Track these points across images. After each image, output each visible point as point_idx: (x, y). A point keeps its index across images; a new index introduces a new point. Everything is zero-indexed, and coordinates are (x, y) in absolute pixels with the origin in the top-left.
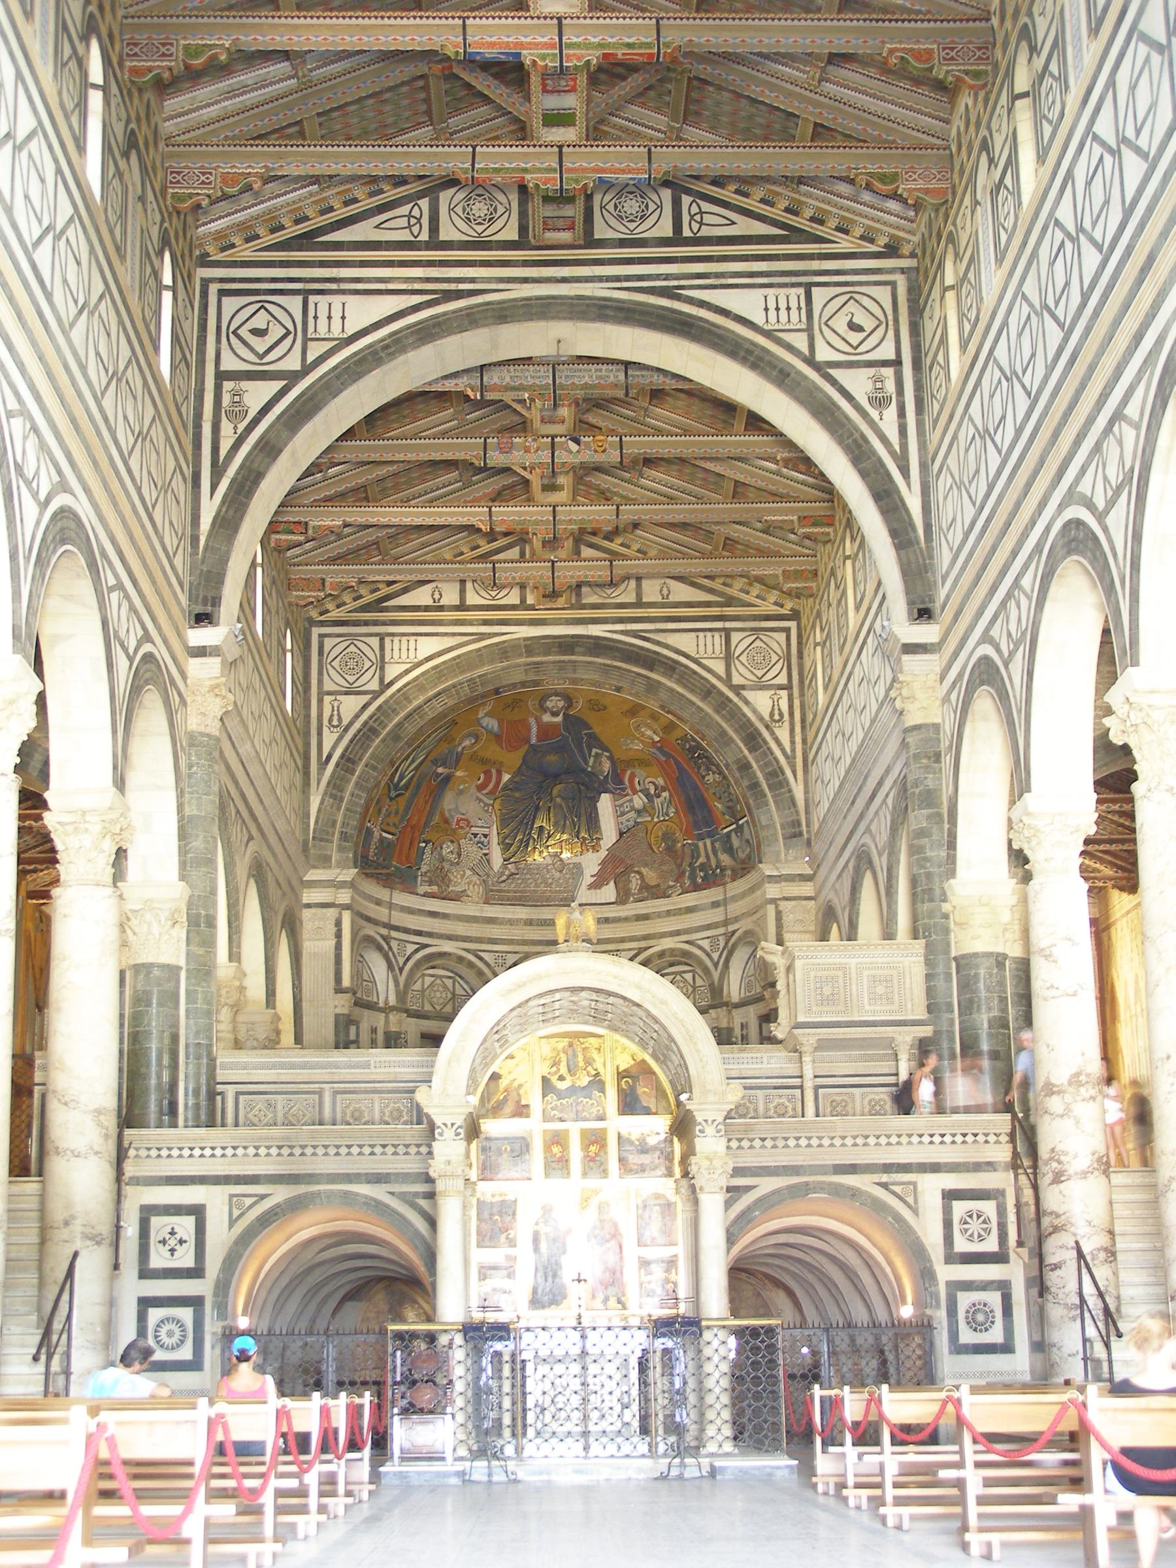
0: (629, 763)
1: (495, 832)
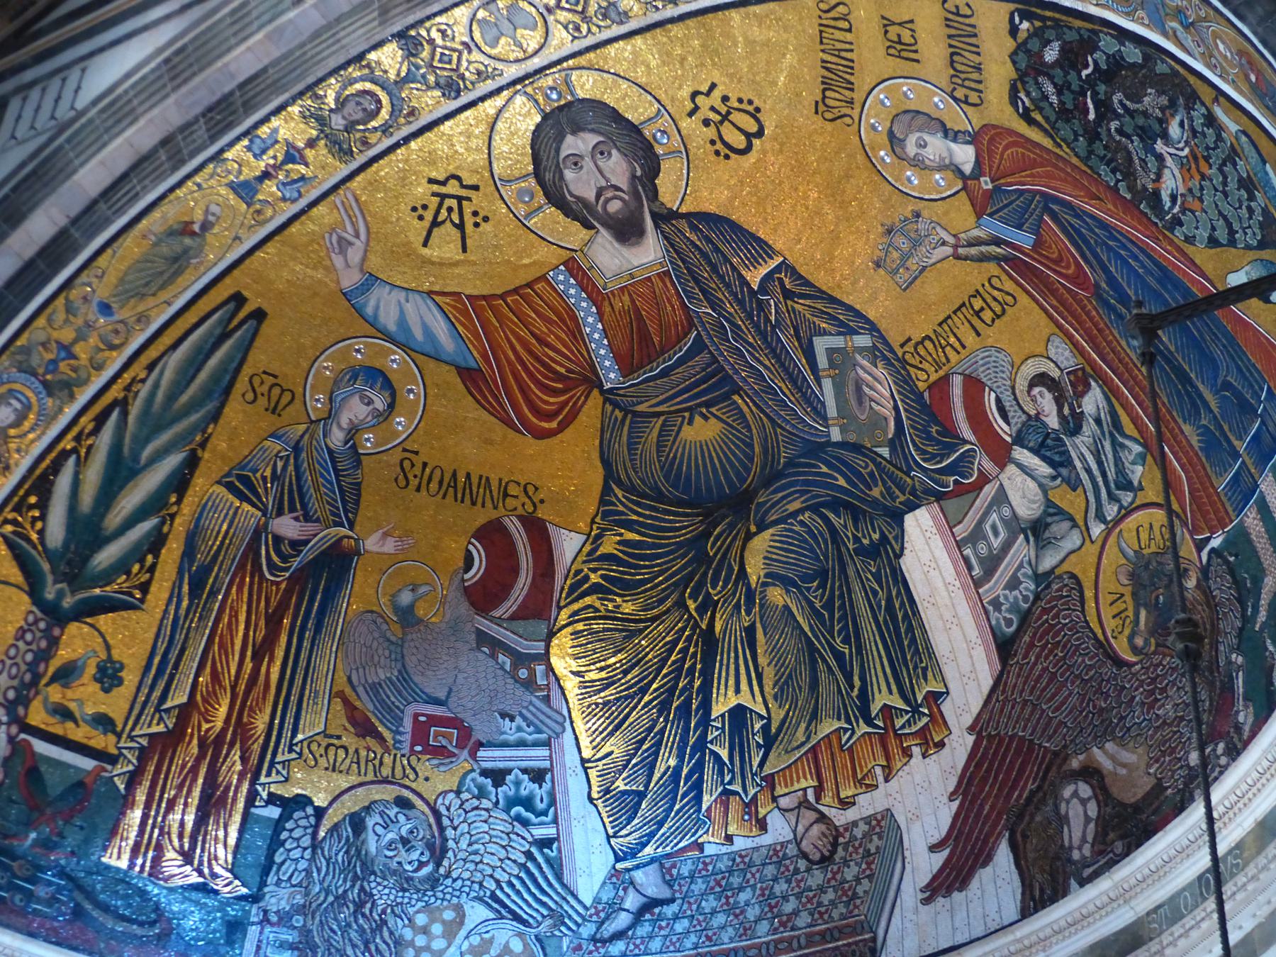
1: (572, 759)
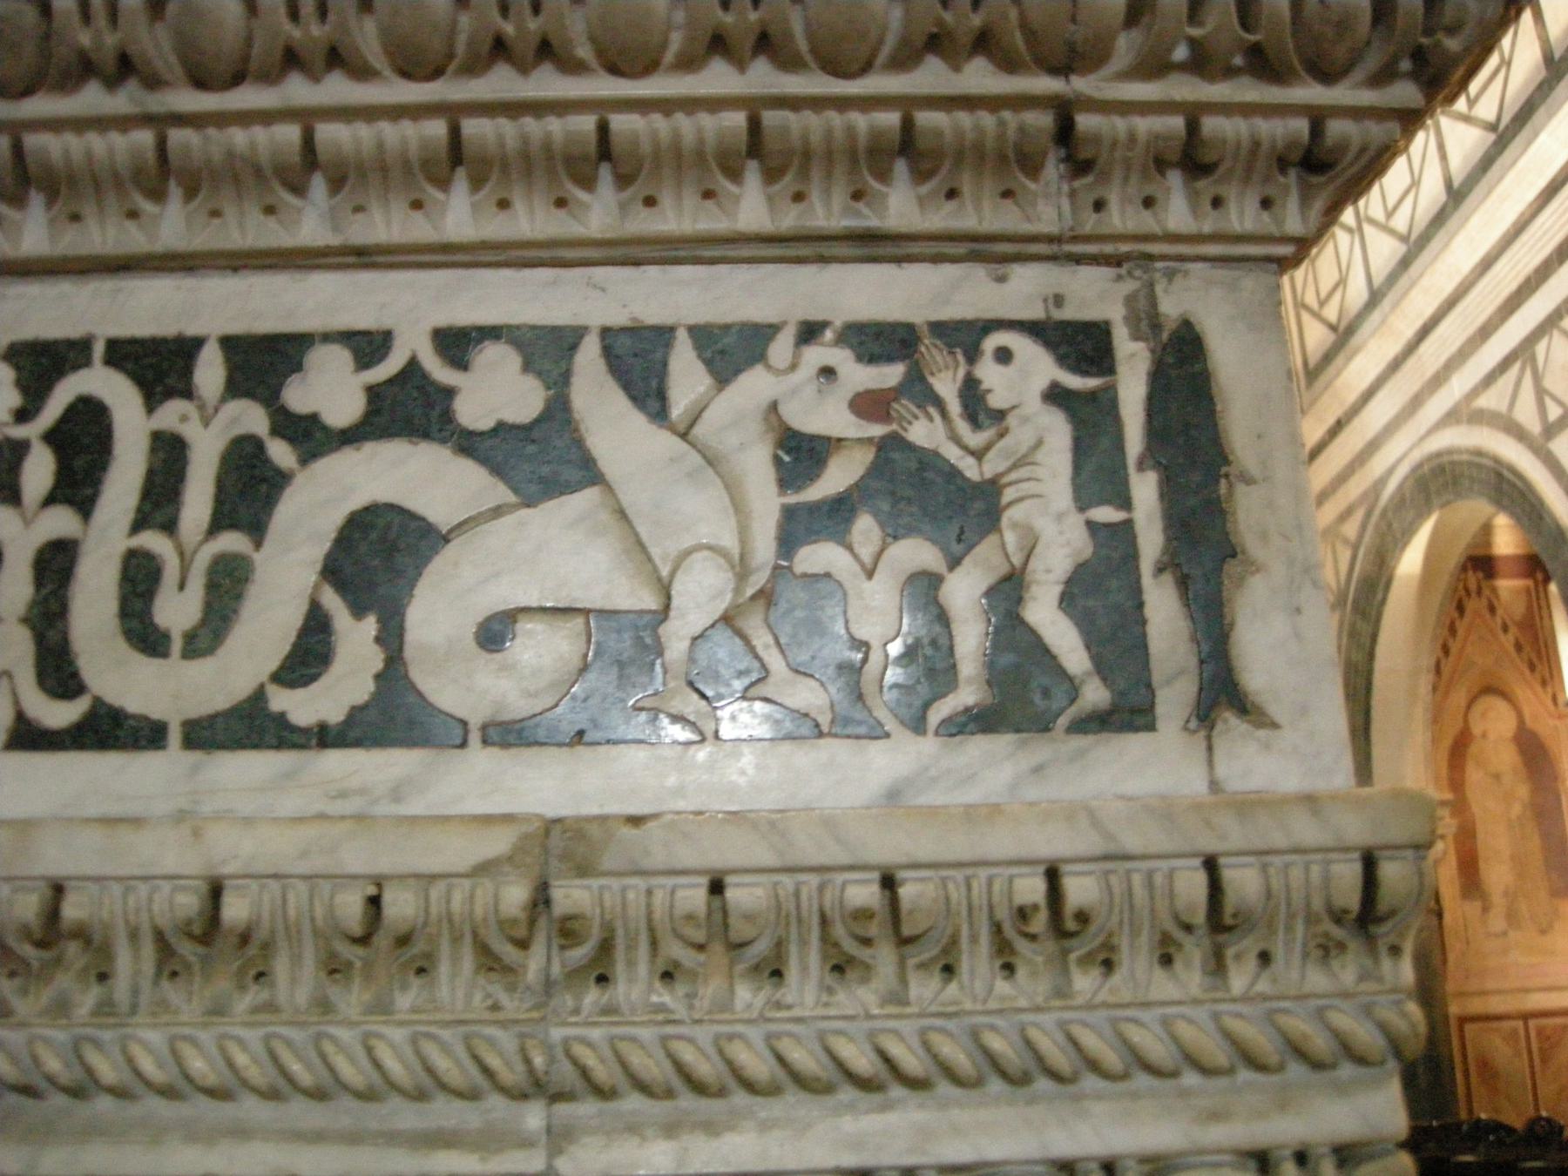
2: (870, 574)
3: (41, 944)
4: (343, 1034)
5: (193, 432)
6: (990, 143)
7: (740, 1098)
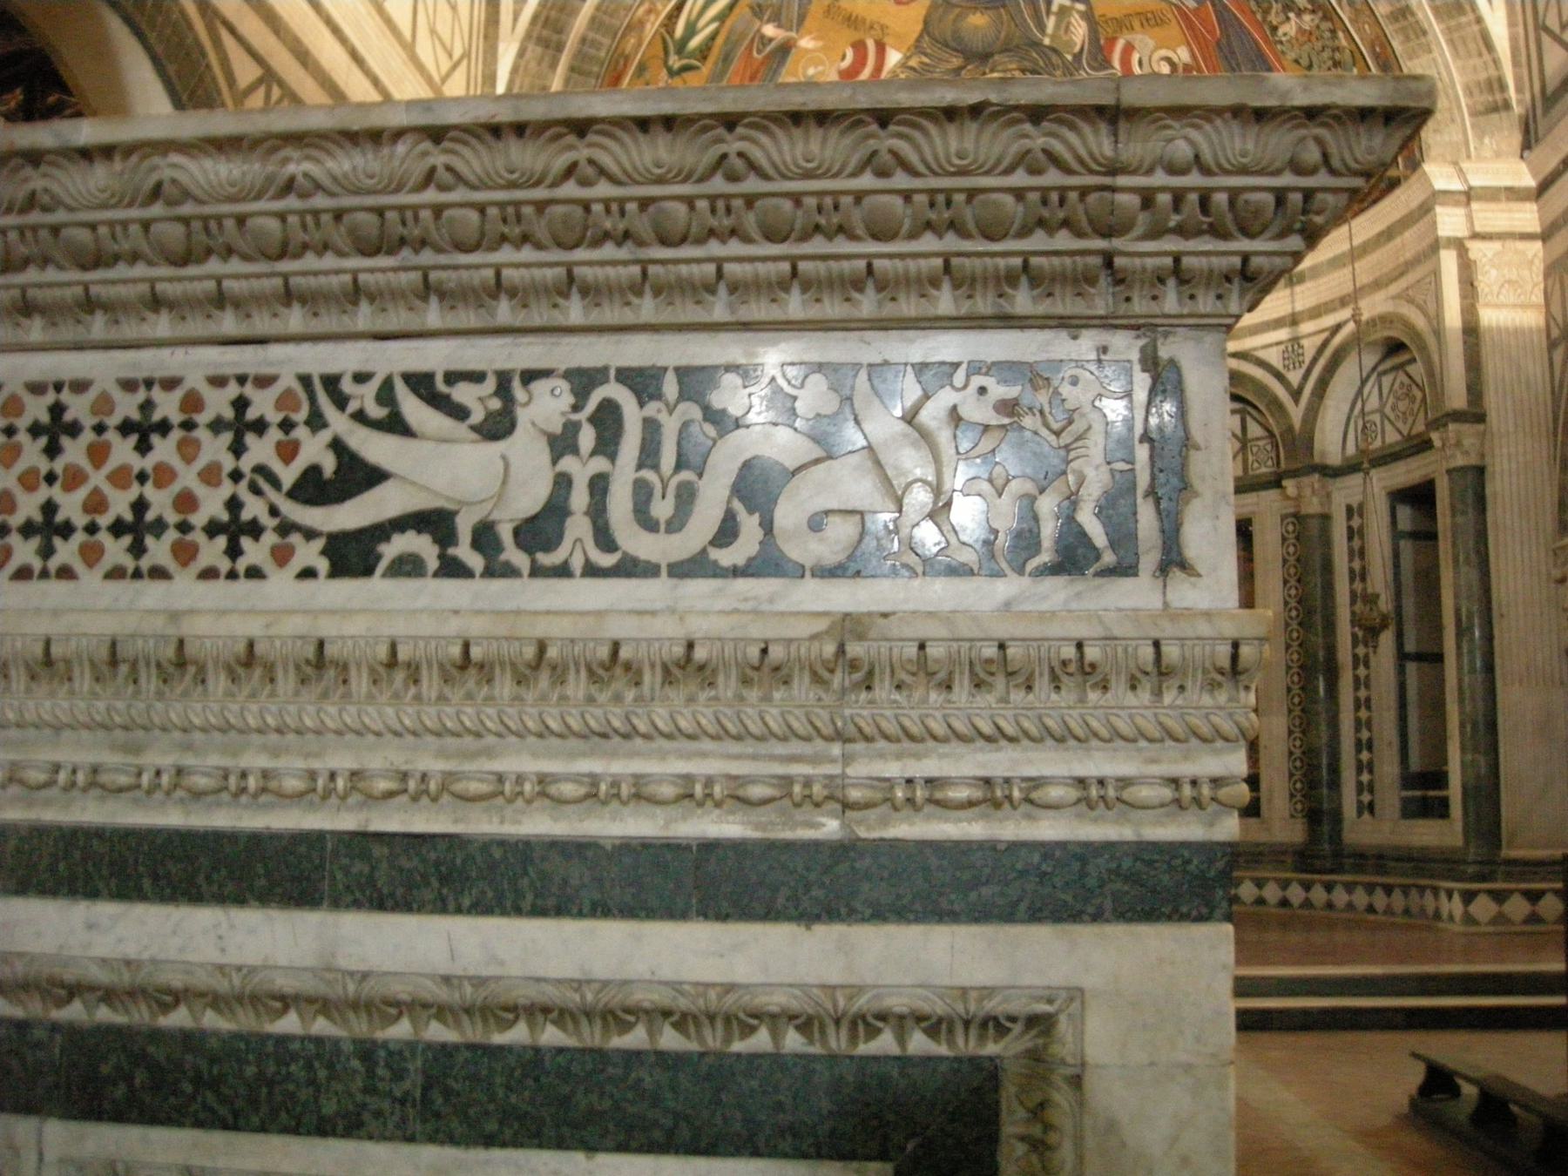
0: (1122, 24)
2: (1000, 495)
3: (607, 669)
4: (749, 711)
5: (663, 417)
6: (1069, 271)
7: (931, 744)
